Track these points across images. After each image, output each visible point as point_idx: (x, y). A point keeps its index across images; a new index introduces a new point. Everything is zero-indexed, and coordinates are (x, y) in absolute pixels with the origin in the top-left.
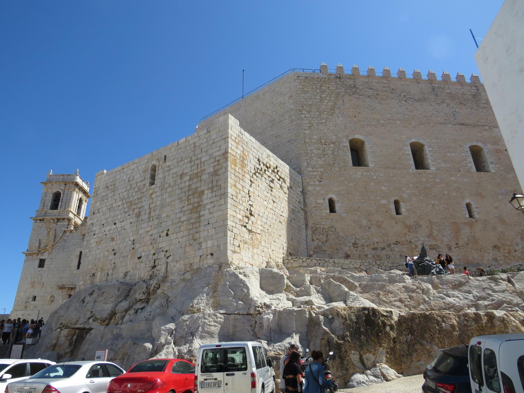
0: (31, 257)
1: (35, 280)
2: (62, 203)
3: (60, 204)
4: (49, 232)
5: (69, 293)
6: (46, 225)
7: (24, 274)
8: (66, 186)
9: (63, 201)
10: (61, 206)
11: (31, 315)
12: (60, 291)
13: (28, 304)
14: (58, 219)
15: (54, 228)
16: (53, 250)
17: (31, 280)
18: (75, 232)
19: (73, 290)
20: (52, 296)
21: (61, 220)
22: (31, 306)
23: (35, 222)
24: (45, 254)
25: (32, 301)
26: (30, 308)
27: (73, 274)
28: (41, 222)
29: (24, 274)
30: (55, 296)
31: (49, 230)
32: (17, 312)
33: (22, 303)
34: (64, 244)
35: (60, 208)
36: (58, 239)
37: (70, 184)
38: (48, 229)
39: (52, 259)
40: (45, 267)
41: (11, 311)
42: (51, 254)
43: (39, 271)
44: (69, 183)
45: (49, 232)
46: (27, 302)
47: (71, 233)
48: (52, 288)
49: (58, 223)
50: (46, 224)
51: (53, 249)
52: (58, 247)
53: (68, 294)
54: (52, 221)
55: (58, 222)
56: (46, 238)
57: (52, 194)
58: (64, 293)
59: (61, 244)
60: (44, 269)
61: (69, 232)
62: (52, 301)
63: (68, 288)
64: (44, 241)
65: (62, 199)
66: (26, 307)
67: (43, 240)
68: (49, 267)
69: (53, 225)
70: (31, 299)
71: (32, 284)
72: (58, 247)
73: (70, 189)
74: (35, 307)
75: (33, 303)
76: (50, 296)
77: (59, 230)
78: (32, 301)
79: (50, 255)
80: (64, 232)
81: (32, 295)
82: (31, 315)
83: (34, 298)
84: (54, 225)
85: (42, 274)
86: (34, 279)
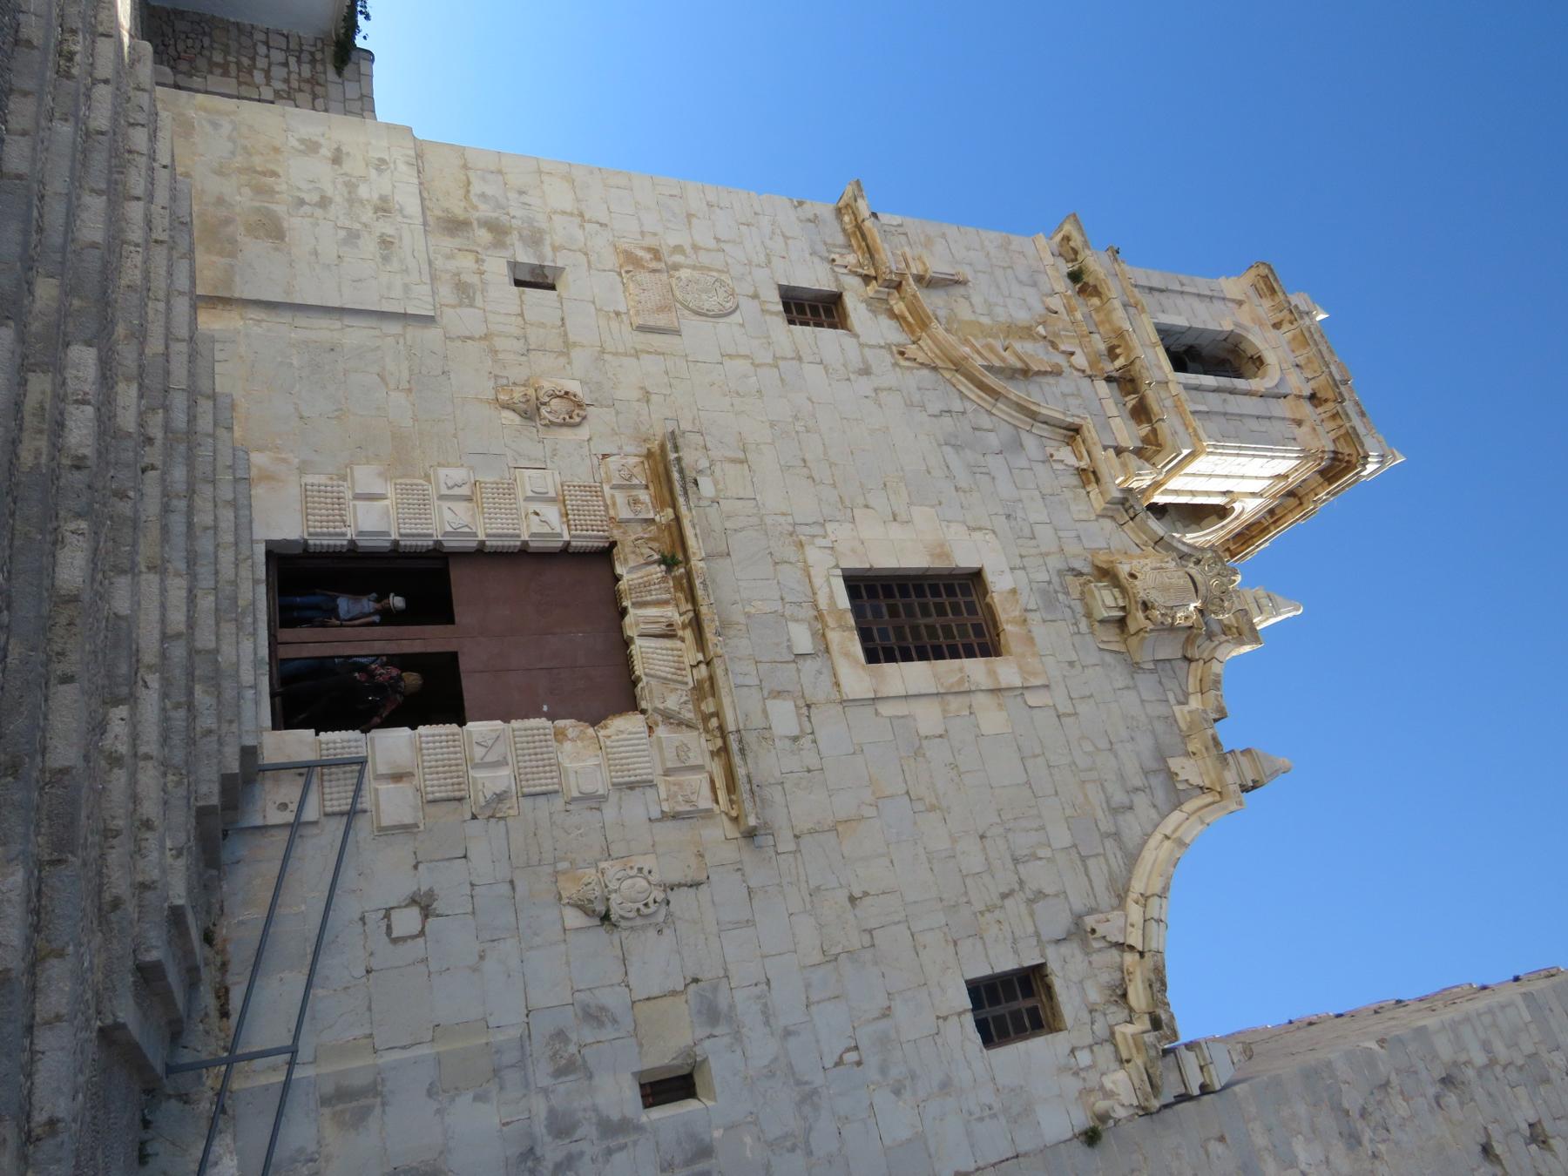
0: (841, 239)
1: (684, 273)
2: (1217, 390)
3: (1209, 380)
4: (1027, 333)
5: (627, 539)
6: (1062, 310)
7: (710, 205)
8: (1307, 409)
9: (1231, 398)
10: (1197, 388)
11: (386, 259)
12: (628, 460)
13: (484, 235)
14: (1132, 380)
15: (1061, 360)
16: (925, 372)
17: (678, 249)
18: (1098, 503)
19: (658, 571)
20: (580, 405)
21: (1132, 400)
22: (467, 262)
23: (1057, 253)
24: (885, 322)
25: (514, 266)
26: (450, 257)
27: (801, 545)
28: (1068, 281)
29: (710, 205)
30: (583, 432)
31: (1041, 329)
32: (402, 167)
33: (483, 196)
34: (993, 440)
35: (1187, 387)
36: (1015, 391)
37: (1332, 425)
38: (1044, 323)
39: (866, 371)
40: (797, 329)
41: (410, 130)
42: (896, 364)
43: (755, 296)
44: (1335, 416)
45: (1027, 333)
46: (498, 231)
47: (1075, 481)
48: (647, 396)
49: (1102, 387)
50: (1070, 310)
51: (935, 369)
52: (957, 405)
53: (616, 534)
54: (1102, 347)
55: (1109, 379)
56: (985, 320)
57: (1238, 331)
58: (620, 498)
59: (986, 421)
60: (778, 324)
61: (1083, 464)
62: (530, 412)
63: (678, 519)
64: (964, 313)
65: (1233, 392)
66: (455, 226)
67: (967, 298)
68: (800, 359)
69: (1078, 351)
70: (525, 257)
71: (648, 256)
72: (957, 405)
73: (1305, 429)
74: (465, 292)
75: (497, 268)
76: (573, 386)
77: (1064, 395)
78: (514, 266)
79: (888, 359)
80: (1067, 429)
81: (560, 264)
82: (386, 259)
83: (536, 279)
84: (1080, 360)
85: (736, 317)
86: (694, 268)
